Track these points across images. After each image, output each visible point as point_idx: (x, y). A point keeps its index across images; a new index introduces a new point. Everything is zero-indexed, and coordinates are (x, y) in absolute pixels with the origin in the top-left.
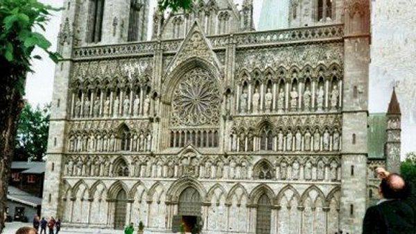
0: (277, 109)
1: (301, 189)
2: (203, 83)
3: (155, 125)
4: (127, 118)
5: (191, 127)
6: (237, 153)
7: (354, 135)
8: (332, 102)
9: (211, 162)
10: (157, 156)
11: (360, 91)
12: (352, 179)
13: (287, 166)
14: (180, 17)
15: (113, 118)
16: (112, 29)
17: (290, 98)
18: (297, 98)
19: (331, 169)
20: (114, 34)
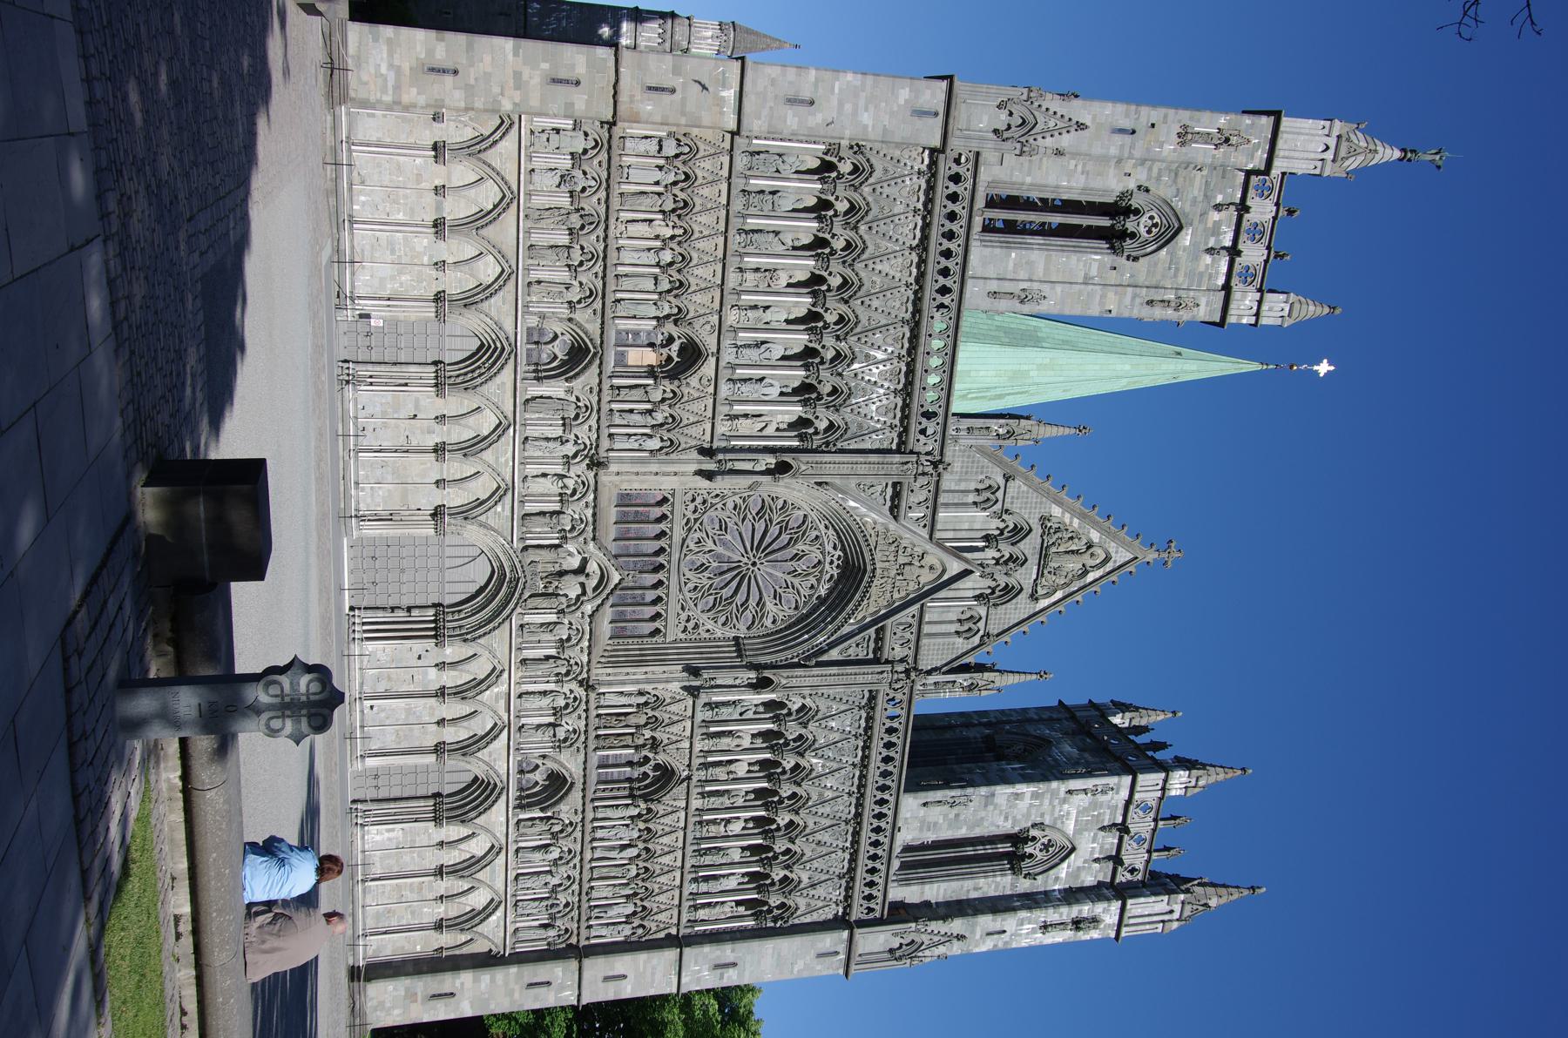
0: (703, 795)
1: (493, 871)
2: (796, 581)
3: (693, 462)
4: (722, 364)
5: (676, 556)
6: (593, 713)
7: (625, 977)
8: (707, 910)
9: (569, 639)
10: (591, 475)
11: (726, 975)
12: (517, 987)
13: (554, 836)
14: (997, 501)
15: (727, 307)
16: (1008, 287)
17: (728, 821)
18: (726, 837)
19: (545, 926)
20: (994, 294)
